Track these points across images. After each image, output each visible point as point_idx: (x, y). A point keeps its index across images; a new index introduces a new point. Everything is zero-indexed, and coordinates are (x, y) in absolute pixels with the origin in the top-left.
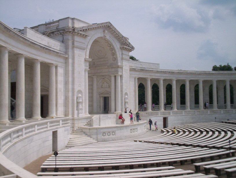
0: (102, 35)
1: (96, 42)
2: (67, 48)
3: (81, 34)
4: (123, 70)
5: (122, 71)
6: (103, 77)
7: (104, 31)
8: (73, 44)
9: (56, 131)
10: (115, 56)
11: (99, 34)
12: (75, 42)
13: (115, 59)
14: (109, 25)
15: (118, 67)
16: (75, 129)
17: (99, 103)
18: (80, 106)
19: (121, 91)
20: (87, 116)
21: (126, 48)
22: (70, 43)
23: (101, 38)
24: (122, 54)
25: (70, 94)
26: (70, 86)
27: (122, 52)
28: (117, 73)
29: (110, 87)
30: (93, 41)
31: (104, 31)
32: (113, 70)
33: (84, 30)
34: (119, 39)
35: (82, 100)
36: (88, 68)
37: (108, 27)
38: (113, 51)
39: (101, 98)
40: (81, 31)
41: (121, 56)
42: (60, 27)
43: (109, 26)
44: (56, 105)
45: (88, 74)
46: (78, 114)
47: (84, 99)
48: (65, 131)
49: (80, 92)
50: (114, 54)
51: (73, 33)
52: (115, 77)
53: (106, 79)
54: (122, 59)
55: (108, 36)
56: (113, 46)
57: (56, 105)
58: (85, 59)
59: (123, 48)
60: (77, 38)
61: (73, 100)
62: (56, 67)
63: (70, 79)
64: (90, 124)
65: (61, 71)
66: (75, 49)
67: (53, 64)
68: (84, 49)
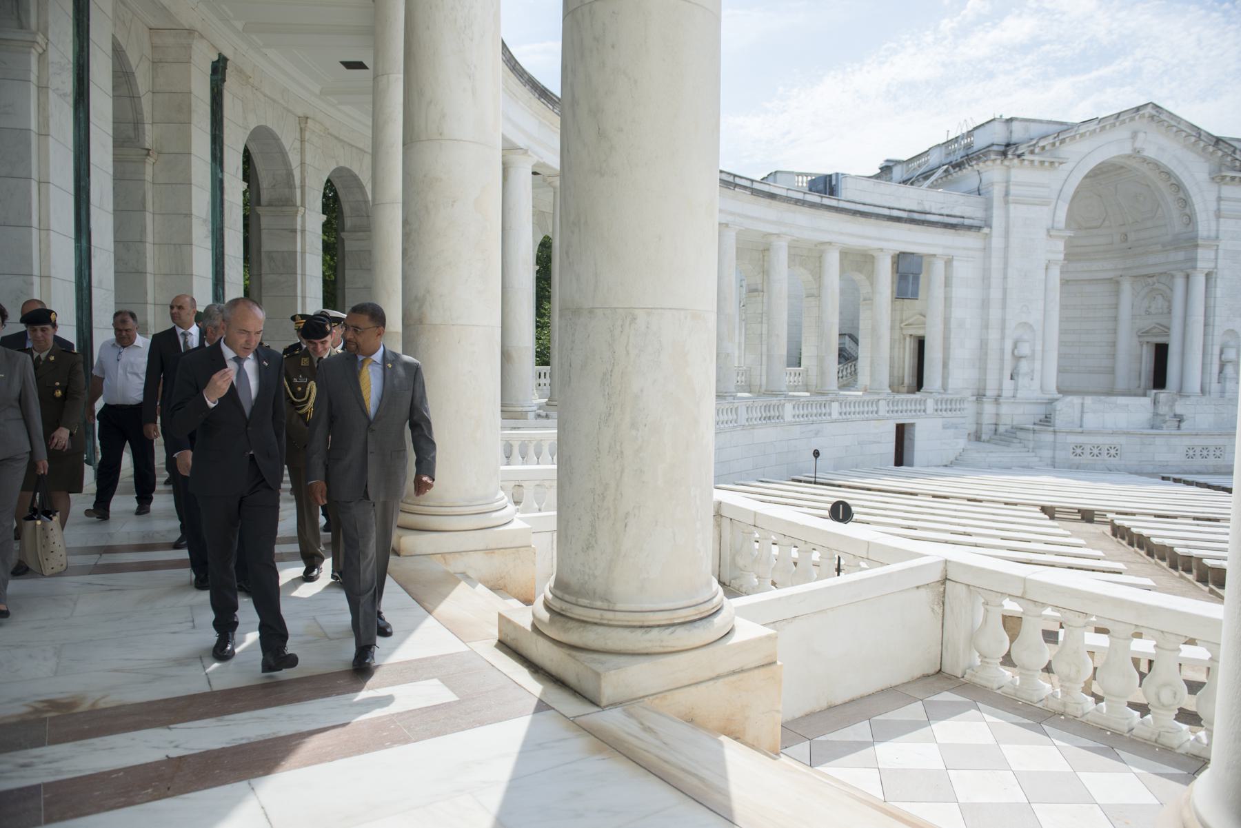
0: (1127, 149)
1: (1102, 174)
2: (988, 207)
3: (1032, 162)
4: (1221, 252)
5: (1216, 259)
6: (1150, 280)
7: (1134, 135)
8: (1007, 194)
9: (913, 425)
10: (1187, 211)
11: (1111, 148)
12: (1012, 187)
13: (1190, 219)
14: (1154, 112)
15: (1197, 246)
16: (1001, 429)
17: (1132, 359)
18: (1024, 366)
19: (1206, 325)
20: (1048, 396)
21: (1233, 178)
22: (997, 192)
23: (1129, 156)
24: (1219, 199)
25: (994, 335)
26: (995, 313)
27: (1219, 191)
28: (1195, 268)
29: (1170, 312)
30: (1086, 172)
31: (1134, 135)
32: (1181, 255)
33: (1043, 148)
34: (1204, 149)
35: (1033, 351)
36: (1062, 256)
37: (1153, 114)
38: (1181, 195)
39: (1145, 346)
40: (1032, 152)
41: (1213, 206)
42: (976, 148)
43: (1152, 117)
44: (945, 365)
45: (1061, 272)
46: (1016, 389)
47: (1039, 348)
48: (945, 427)
49: (1025, 324)
50: (1185, 202)
51: (1006, 163)
52: (1188, 277)
53: (1161, 286)
54: (1218, 215)
55: (1158, 146)
56: (1176, 178)
57: (945, 365)
58: (1048, 231)
59: (1223, 178)
60: (1022, 175)
61: (1002, 351)
62: (949, 262)
63: (995, 294)
64: (1047, 420)
65: (965, 270)
66: (1012, 207)
67: (934, 255)
68: (1044, 203)
